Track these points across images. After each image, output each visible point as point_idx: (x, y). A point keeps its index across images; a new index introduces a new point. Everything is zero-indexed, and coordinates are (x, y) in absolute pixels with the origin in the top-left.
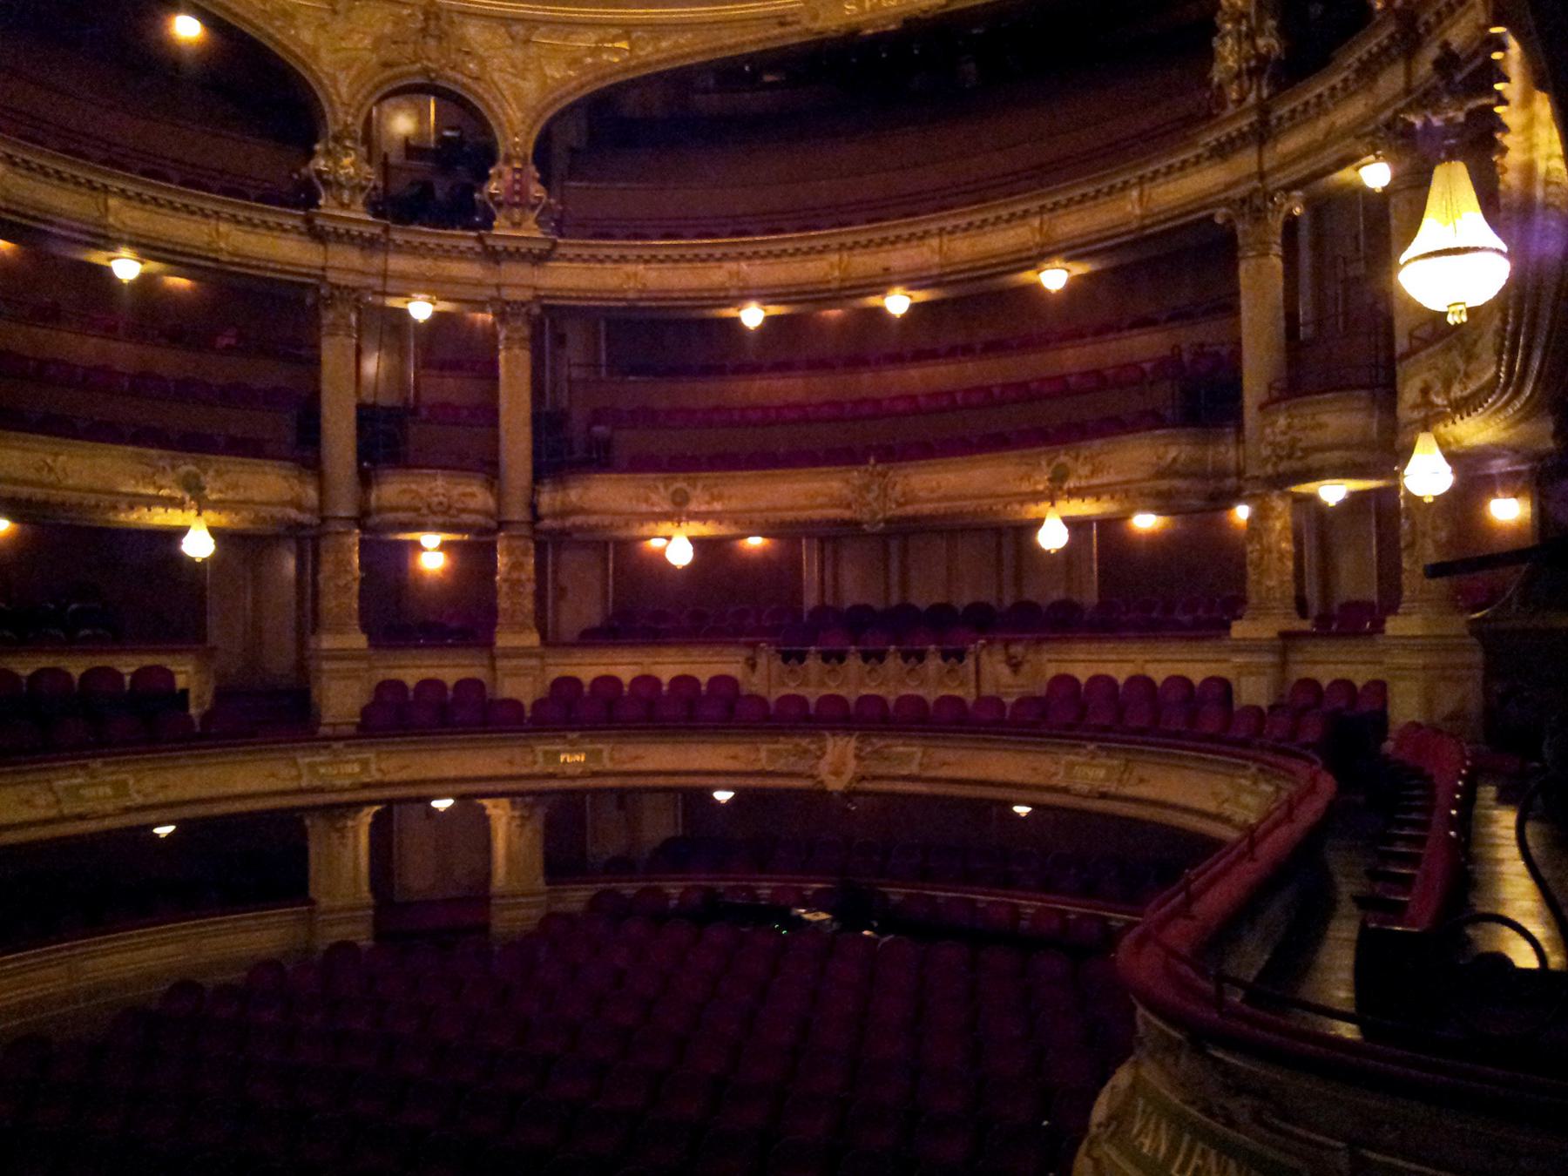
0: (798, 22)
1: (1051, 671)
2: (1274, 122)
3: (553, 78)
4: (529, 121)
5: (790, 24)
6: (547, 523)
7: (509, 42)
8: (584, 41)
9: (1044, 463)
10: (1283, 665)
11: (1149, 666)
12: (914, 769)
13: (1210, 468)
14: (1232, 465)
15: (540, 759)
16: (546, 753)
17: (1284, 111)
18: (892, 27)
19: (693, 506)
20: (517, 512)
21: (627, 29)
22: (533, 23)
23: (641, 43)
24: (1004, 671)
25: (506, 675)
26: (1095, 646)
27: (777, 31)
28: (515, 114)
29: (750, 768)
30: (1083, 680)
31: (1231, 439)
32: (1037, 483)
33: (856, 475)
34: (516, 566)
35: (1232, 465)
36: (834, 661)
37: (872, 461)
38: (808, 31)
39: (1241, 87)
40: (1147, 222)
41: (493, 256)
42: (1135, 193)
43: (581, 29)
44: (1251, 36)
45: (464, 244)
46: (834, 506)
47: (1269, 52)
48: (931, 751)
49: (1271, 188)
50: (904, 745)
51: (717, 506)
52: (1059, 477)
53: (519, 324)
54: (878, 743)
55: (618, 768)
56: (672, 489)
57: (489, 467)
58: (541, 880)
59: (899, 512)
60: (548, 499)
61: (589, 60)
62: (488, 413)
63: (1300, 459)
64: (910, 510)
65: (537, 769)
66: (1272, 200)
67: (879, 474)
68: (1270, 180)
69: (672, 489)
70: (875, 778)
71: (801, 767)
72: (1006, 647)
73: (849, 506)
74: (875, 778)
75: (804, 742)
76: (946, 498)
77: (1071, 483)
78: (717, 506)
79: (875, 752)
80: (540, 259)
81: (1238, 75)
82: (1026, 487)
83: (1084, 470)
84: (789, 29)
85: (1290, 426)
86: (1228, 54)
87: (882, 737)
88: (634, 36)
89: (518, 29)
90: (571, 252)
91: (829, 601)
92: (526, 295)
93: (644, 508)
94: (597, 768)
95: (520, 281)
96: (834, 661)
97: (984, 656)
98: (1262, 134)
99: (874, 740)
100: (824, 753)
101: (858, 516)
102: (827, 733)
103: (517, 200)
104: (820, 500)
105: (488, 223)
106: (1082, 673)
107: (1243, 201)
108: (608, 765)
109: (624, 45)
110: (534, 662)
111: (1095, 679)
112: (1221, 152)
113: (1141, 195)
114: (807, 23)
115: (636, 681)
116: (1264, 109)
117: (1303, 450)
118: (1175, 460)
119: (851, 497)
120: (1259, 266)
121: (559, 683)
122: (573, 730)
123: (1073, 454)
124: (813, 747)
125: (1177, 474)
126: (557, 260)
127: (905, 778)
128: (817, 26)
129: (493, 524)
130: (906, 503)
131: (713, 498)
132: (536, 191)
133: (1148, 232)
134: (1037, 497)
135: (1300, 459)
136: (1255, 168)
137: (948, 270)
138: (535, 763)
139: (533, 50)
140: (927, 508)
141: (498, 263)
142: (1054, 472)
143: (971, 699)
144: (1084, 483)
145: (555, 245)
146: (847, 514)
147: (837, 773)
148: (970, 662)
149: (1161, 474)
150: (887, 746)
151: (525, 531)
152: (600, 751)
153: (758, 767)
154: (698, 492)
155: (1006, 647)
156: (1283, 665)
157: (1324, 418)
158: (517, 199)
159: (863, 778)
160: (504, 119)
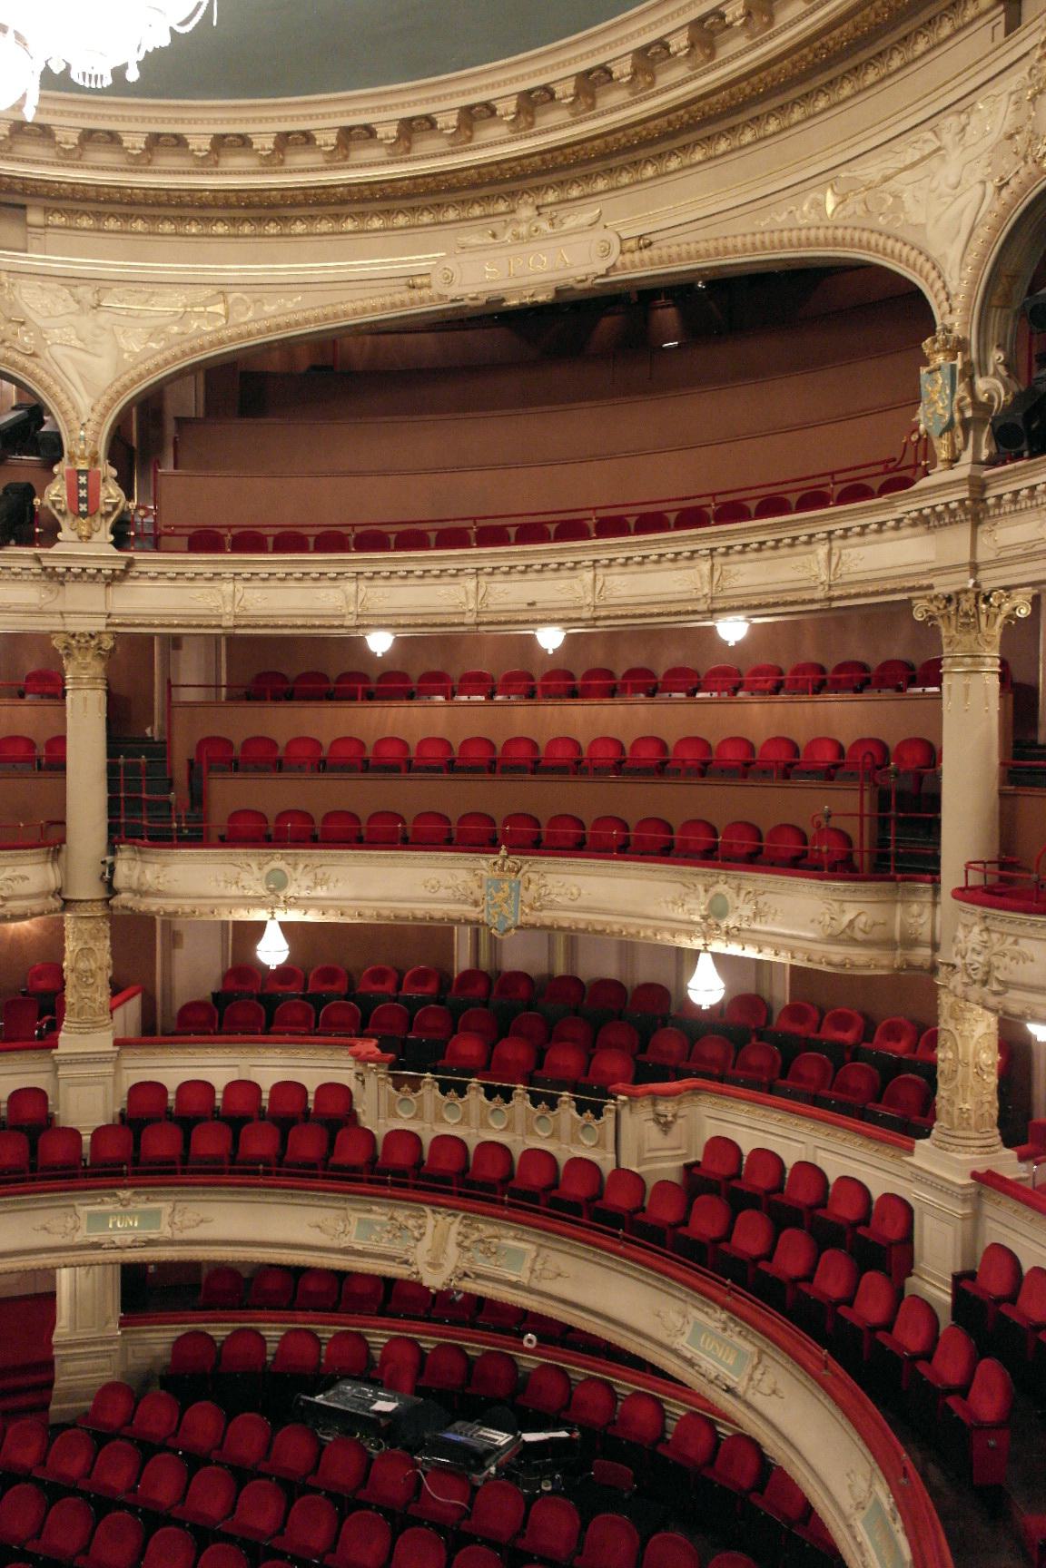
0: (429, 286)
1: (711, 1130)
2: (991, 501)
3: (131, 353)
4: (99, 408)
5: (421, 287)
6: (124, 898)
7: (75, 307)
8: (167, 305)
9: (701, 888)
10: (976, 1217)
11: (821, 1153)
12: (523, 1276)
13: (897, 936)
14: (925, 933)
15: (84, 1223)
16: (91, 1215)
17: (1005, 489)
18: (541, 298)
19: (291, 891)
20: (86, 887)
21: (222, 290)
22: (101, 284)
23: (242, 308)
24: (652, 1130)
25: (69, 1085)
26: (760, 1111)
27: (407, 296)
28: (84, 402)
29: (335, 1244)
30: (746, 1150)
31: (928, 898)
32: (690, 912)
33: (484, 864)
34: (86, 952)
35: (925, 933)
36: (452, 1093)
37: (503, 852)
38: (441, 297)
39: (953, 444)
40: (836, 593)
41: (55, 578)
42: (822, 550)
43: (168, 290)
44: (968, 374)
45: (17, 565)
46: (459, 901)
47: (991, 398)
48: (545, 1252)
49: (986, 587)
50: (515, 1238)
51: (321, 892)
52: (717, 910)
53: (89, 659)
55: (179, 1236)
56: (267, 869)
57: (49, 836)
58: (114, 1324)
60: (129, 869)
61: (175, 329)
62: (54, 760)
63: (996, 993)
65: (79, 1238)
66: (986, 600)
67: (510, 870)
68: (982, 575)
69: (267, 869)
71: (396, 1248)
72: (654, 1104)
73: (476, 904)
75: (401, 1215)
77: (730, 922)
78: (321, 892)
79: (481, 1241)
80: (114, 579)
81: (950, 426)
82: (679, 913)
84: (416, 294)
85: (985, 945)
86: (938, 401)
88: (231, 298)
89: (85, 292)
90: (153, 569)
91: (484, 963)
92: (98, 625)
93: (234, 891)
94: (153, 1234)
95: (86, 610)
96: (452, 1093)
97: (625, 1113)
98: (977, 511)
100: (423, 1235)
101: (484, 917)
102: (427, 1209)
103: (85, 506)
104: (443, 893)
105: (51, 534)
106: (747, 1143)
107: (949, 600)
108: (166, 1232)
109: (219, 309)
110: (109, 1069)
111: (760, 1153)
112: (929, 521)
113: (830, 554)
114: (439, 287)
115: (232, 1087)
116: (978, 487)
117: (1000, 982)
118: (852, 922)
119: (478, 894)
120: (967, 687)
121: (139, 1090)
122: (125, 1187)
123: (734, 883)
124: (411, 1223)
125: (853, 942)
126: (136, 578)
127: (515, 1285)
128: (453, 292)
129: (57, 904)
130: (542, 908)
131: (317, 882)
132: (111, 493)
133: (835, 604)
134: (689, 929)
135: (996, 993)
136: (966, 558)
137: (603, 613)
138: (76, 1229)
139: (103, 318)
141: (62, 584)
142: (711, 902)
143: (607, 1167)
145: (130, 563)
147: (435, 1265)
148: (608, 1118)
151: (99, 911)
152: (158, 1212)
153: (344, 1242)
154: (297, 874)
155: (654, 1104)
156: (976, 1217)
157: (1026, 946)
158: (83, 507)
160: (67, 405)
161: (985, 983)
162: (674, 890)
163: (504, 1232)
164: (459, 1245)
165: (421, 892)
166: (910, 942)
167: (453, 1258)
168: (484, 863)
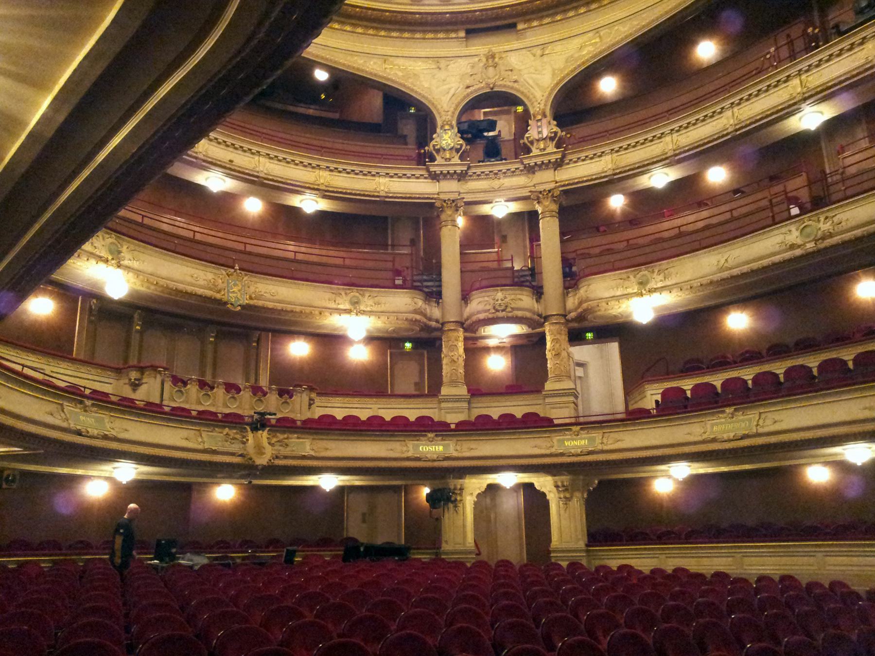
29: (200, 447)
33: (223, 271)
46: (211, 289)
50: (298, 438)
54: (281, 436)
59: (252, 302)
64: (260, 303)
70: (286, 457)
74: (286, 457)
76: (280, 302)
81: (451, 149)
82: (334, 306)
83: (371, 302)
87: (284, 432)
99: (278, 434)
100: (248, 440)
104: (202, 282)
124: (238, 436)
140: (270, 305)
144: (368, 309)
146: (218, 296)
149: (415, 312)
150: (287, 438)
159: (277, 457)
161: (503, 311)
162: (328, 295)
163: (290, 436)
164: (269, 443)
165: (189, 279)
166: (430, 319)
167: (269, 452)
168: (224, 272)
